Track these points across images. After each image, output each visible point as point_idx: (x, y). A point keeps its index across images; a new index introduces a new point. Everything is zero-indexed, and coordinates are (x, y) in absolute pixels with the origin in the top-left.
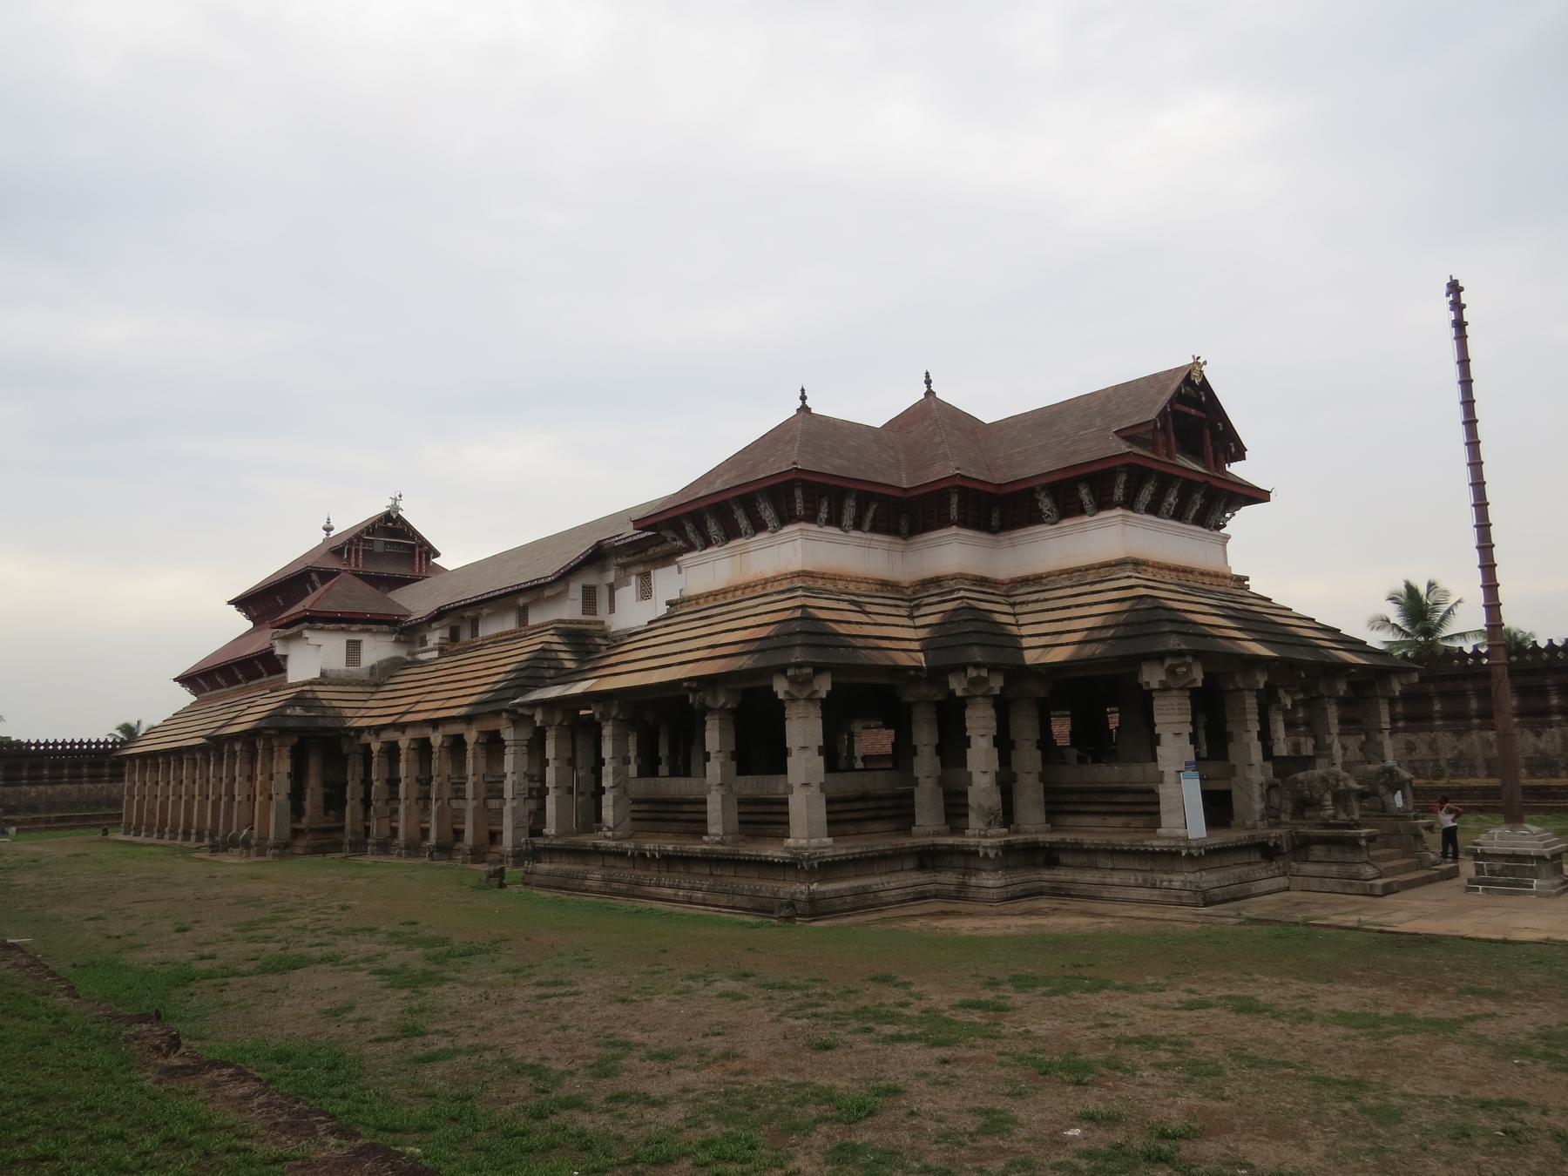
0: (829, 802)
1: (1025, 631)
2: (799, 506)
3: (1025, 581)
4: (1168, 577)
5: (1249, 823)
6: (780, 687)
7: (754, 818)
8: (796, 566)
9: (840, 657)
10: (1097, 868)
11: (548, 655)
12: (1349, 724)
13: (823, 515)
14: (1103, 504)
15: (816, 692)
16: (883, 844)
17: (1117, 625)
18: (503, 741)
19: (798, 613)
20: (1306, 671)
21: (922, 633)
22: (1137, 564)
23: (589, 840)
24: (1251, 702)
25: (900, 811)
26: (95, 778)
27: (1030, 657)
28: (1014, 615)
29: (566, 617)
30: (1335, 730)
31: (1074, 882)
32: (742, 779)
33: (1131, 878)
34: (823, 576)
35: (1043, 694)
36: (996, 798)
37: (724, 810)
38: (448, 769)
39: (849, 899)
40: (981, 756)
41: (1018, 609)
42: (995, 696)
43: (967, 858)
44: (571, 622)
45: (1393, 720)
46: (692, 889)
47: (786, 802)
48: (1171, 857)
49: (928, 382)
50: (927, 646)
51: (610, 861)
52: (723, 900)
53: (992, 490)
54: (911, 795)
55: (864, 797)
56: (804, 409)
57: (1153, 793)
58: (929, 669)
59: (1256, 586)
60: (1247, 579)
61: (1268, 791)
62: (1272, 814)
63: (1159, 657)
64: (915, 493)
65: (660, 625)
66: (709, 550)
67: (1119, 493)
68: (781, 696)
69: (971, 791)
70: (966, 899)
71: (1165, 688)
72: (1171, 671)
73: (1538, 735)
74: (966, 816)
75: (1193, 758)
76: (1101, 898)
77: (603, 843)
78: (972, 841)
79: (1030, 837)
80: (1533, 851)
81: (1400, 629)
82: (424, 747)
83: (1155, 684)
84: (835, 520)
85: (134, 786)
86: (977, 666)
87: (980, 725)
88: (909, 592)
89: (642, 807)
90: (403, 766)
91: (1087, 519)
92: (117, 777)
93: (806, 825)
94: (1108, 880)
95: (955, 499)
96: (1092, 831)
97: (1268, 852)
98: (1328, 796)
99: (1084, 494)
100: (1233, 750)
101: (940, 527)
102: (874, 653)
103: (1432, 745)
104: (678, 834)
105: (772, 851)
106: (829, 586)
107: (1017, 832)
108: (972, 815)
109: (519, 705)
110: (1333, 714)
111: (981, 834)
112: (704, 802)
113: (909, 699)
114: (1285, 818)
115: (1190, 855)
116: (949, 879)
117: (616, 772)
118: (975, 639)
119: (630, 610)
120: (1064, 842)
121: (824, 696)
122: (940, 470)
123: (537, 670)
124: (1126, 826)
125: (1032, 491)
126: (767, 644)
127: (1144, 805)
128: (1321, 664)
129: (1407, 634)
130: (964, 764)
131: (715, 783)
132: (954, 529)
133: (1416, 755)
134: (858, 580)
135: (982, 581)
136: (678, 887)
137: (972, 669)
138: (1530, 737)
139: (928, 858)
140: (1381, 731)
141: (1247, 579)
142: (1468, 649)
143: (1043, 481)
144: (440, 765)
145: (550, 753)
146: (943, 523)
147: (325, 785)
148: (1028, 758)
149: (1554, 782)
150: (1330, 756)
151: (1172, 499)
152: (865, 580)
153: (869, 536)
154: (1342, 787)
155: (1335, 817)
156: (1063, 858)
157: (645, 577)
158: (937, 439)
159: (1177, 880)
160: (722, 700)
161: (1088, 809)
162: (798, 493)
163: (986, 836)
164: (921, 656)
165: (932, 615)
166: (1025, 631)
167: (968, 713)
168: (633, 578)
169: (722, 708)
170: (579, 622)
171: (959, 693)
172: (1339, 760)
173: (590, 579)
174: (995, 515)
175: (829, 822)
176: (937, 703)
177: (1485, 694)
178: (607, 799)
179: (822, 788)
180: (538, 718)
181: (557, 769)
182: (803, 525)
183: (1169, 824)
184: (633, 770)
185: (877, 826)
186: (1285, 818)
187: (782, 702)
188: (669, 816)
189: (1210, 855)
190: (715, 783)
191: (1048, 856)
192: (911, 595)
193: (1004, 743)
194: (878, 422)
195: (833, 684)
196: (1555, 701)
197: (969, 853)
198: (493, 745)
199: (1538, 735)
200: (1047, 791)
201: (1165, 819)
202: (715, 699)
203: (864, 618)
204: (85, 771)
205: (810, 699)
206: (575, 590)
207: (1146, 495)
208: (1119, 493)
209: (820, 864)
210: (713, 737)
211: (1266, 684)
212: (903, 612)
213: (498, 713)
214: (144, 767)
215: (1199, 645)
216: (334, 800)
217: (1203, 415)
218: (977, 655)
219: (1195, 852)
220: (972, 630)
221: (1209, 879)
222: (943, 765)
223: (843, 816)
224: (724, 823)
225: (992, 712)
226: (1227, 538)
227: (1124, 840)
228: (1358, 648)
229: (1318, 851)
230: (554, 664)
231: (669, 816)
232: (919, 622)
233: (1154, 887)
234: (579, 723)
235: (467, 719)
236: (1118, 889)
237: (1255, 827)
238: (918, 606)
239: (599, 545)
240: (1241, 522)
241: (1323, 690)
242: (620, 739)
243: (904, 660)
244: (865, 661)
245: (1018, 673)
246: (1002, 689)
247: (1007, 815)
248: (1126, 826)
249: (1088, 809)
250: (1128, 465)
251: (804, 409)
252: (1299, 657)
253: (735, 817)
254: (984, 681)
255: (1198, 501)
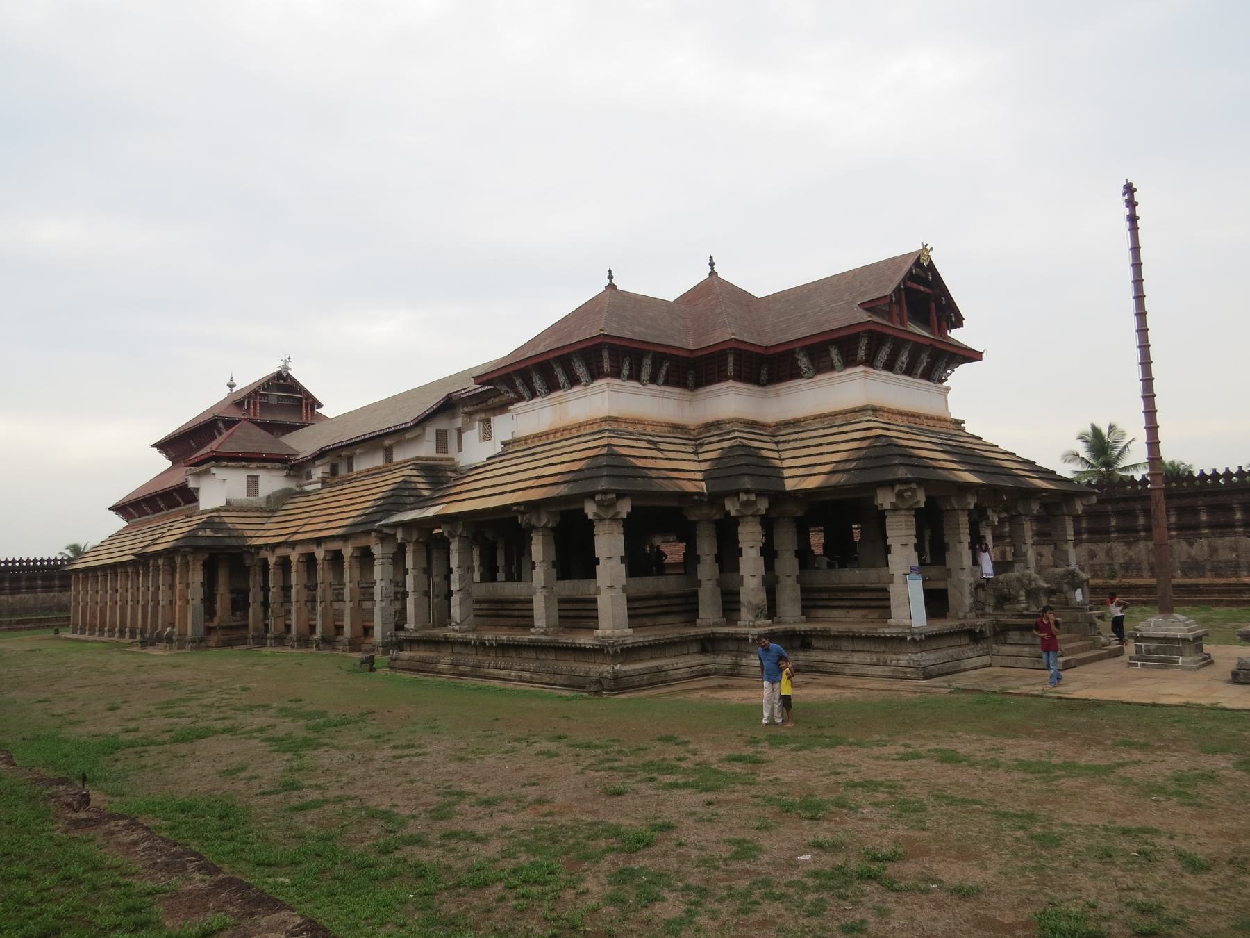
0: (629, 600)
1: (786, 464)
3: (787, 424)
4: (900, 420)
5: (961, 614)
6: (590, 510)
7: (571, 614)
8: (604, 413)
9: (639, 485)
10: (841, 650)
11: (409, 485)
12: (1043, 536)
13: (625, 372)
14: (850, 362)
15: (618, 513)
16: (673, 633)
17: (858, 459)
18: (373, 555)
19: (605, 451)
20: (1007, 497)
21: (704, 466)
22: (875, 410)
23: (440, 633)
24: (964, 520)
25: (688, 606)
26: (48, 588)
27: (790, 485)
28: (778, 451)
29: (423, 455)
30: (1029, 541)
31: (822, 661)
32: (561, 583)
33: (868, 658)
34: (625, 421)
35: (798, 514)
36: (763, 596)
37: (546, 608)
38: (330, 577)
39: (646, 677)
40: (750, 564)
41: (781, 447)
42: (761, 516)
43: (739, 643)
44: (427, 459)
45: (1077, 533)
46: (522, 670)
47: (595, 601)
48: (899, 641)
49: (712, 264)
50: (708, 476)
51: (457, 649)
52: (546, 679)
53: (760, 351)
54: (695, 594)
55: (658, 596)
56: (611, 286)
57: (886, 591)
58: (709, 494)
59: (970, 428)
60: (963, 422)
61: (976, 589)
62: (978, 607)
63: (890, 484)
64: (700, 353)
65: (498, 462)
66: (535, 400)
67: (862, 353)
68: (591, 517)
69: (742, 590)
70: (739, 675)
71: (895, 509)
72: (900, 496)
73: (1191, 545)
74: (739, 610)
75: (916, 563)
76: (844, 674)
77: (452, 634)
78: (743, 630)
79: (789, 627)
80: (1179, 635)
81: (1087, 462)
82: (310, 560)
83: (887, 506)
84: (635, 376)
85: (78, 594)
86: (747, 492)
87: (750, 538)
88: (695, 433)
89: (484, 606)
90: (294, 576)
91: (836, 374)
92: (66, 587)
93: (612, 620)
94: (850, 660)
95: (731, 359)
96: (836, 621)
97: (975, 636)
98: (1022, 593)
99: (834, 354)
100: (949, 557)
101: (720, 381)
102: (664, 482)
103: (1109, 553)
104: (512, 627)
105: (585, 640)
106: (631, 429)
107: (779, 623)
108: (744, 611)
109: (384, 526)
110: (1028, 529)
111: (749, 624)
112: (531, 601)
113: (692, 517)
114: (989, 610)
115: (913, 640)
116: (725, 660)
117: (461, 577)
118: (746, 470)
119: (474, 449)
120: (815, 630)
121: (625, 516)
122: (719, 336)
123: (399, 498)
124: (864, 617)
125: (793, 352)
126: (581, 475)
127: (878, 600)
128: (1019, 489)
129: (1093, 466)
130: (738, 570)
131: (539, 585)
132: (731, 383)
133: (1096, 561)
134: (654, 424)
135: (753, 424)
136: (511, 669)
137: (746, 496)
138: (1185, 546)
139: (709, 644)
140: (1066, 541)
141: (963, 422)
142: (1138, 477)
143: (801, 344)
144: (323, 575)
145: (409, 563)
146: (721, 377)
147: (232, 592)
148: (788, 565)
149: (1201, 581)
150: (1026, 562)
151: (904, 358)
152: (659, 424)
153: (663, 388)
154: (1033, 585)
155: (1027, 609)
156: (815, 643)
157: (487, 422)
158: (718, 310)
159: (903, 659)
160: (544, 521)
161: (836, 603)
162: (605, 354)
163: (754, 626)
164: (703, 483)
165: (712, 451)
166: (786, 464)
167: (740, 529)
168: (477, 423)
169: (545, 527)
170: (434, 459)
171: (733, 513)
172: (1032, 564)
173: (442, 424)
174: (764, 372)
175: (630, 616)
176: (716, 522)
177: (1147, 513)
178: (455, 600)
179: (624, 589)
180: (399, 536)
181: (415, 577)
182: (609, 380)
183: (898, 616)
184: (477, 576)
185: (669, 619)
186: (989, 610)
187: (591, 522)
188: (505, 613)
189: (930, 640)
190: (539, 585)
191: (803, 641)
192: (695, 436)
193: (769, 553)
194: (671, 297)
195: (632, 507)
196: (1204, 518)
197: (740, 640)
198: (365, 557)
199: (1191, 545)
200: (803, 591)
201: (894, 611)
202: (539, 519)
203: (658, 454)
204: (23, 583)
205: (614, 519)
206: (430, 433)
207: (883, 355)
208: (862, 353)
209: (622, 650)
210: (538, 550)
211: (976, 505)
212: (689, 449)
213: (368, 533)
214: (86, 578)
215: (925, 474)
216: (240, 603)
217: (928, 290)
218: (747, 483)
219: (917, 638)
220: (744, 461)
221: (928, 658)
222: (721, 570)
223: (640, 612)
224: (547, 618)
225: (759, 528)
226: (948, 389)
227: (861, 628)
228: (1049, 476)
229: (1014, 636)
230: (414, 492)
231: (505, 613)
232: (702, 457)
233: (885, 665)
234: (430, 540)
235: (344, 538)
236: (854, 667)
237: (965, 617)
238: (702, 445)
239: (449, 397)
240: (959, 376)
241: (1020, 509)
242: (465, 552)
243: (689, 487)
244: (657, 488)
245: (780, 498)
246: (767, 510)
247: (772, 609)
248: (864, 617)
249: (836, 603)
250: (870, 331)
251: (611, 286)
252: (1002, 483)
253: (556, 614)
254: (754, 503)
255: (925, 359)
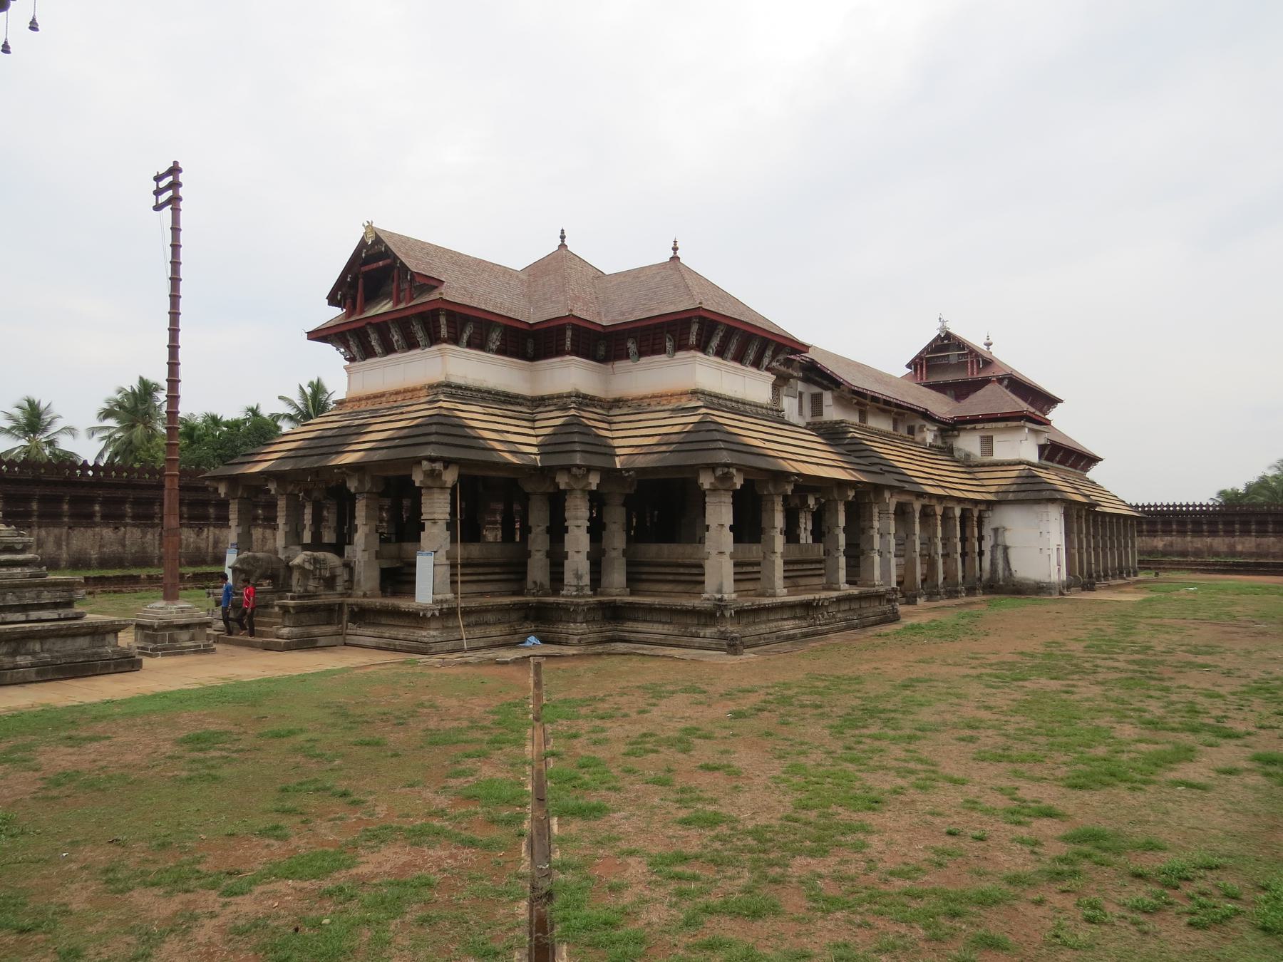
2: (444, 332)
6: (418, 479)
8: (440, 378)
42: (591, 493)
48: (711, 615)
49: (563, 238)
53: (600, 329)
66: (369, 361)
67: (693, 339)
95: (569, 333)
107: (602, 594)
127: (693, 575)
130: (563, 541)
132: (568, 358)
146: (560, 352)
148: (616, 540)
151: (733, 347)
162: (443, 320)
166: (616, 443)
171: (562, 487)
187: (420, 488)
193: (596, 530)
195: (459, 476)
200: (629, 564)
205: (443, 488)
207: (715, 343)
208: (693, 339)
245: (609, 474)
